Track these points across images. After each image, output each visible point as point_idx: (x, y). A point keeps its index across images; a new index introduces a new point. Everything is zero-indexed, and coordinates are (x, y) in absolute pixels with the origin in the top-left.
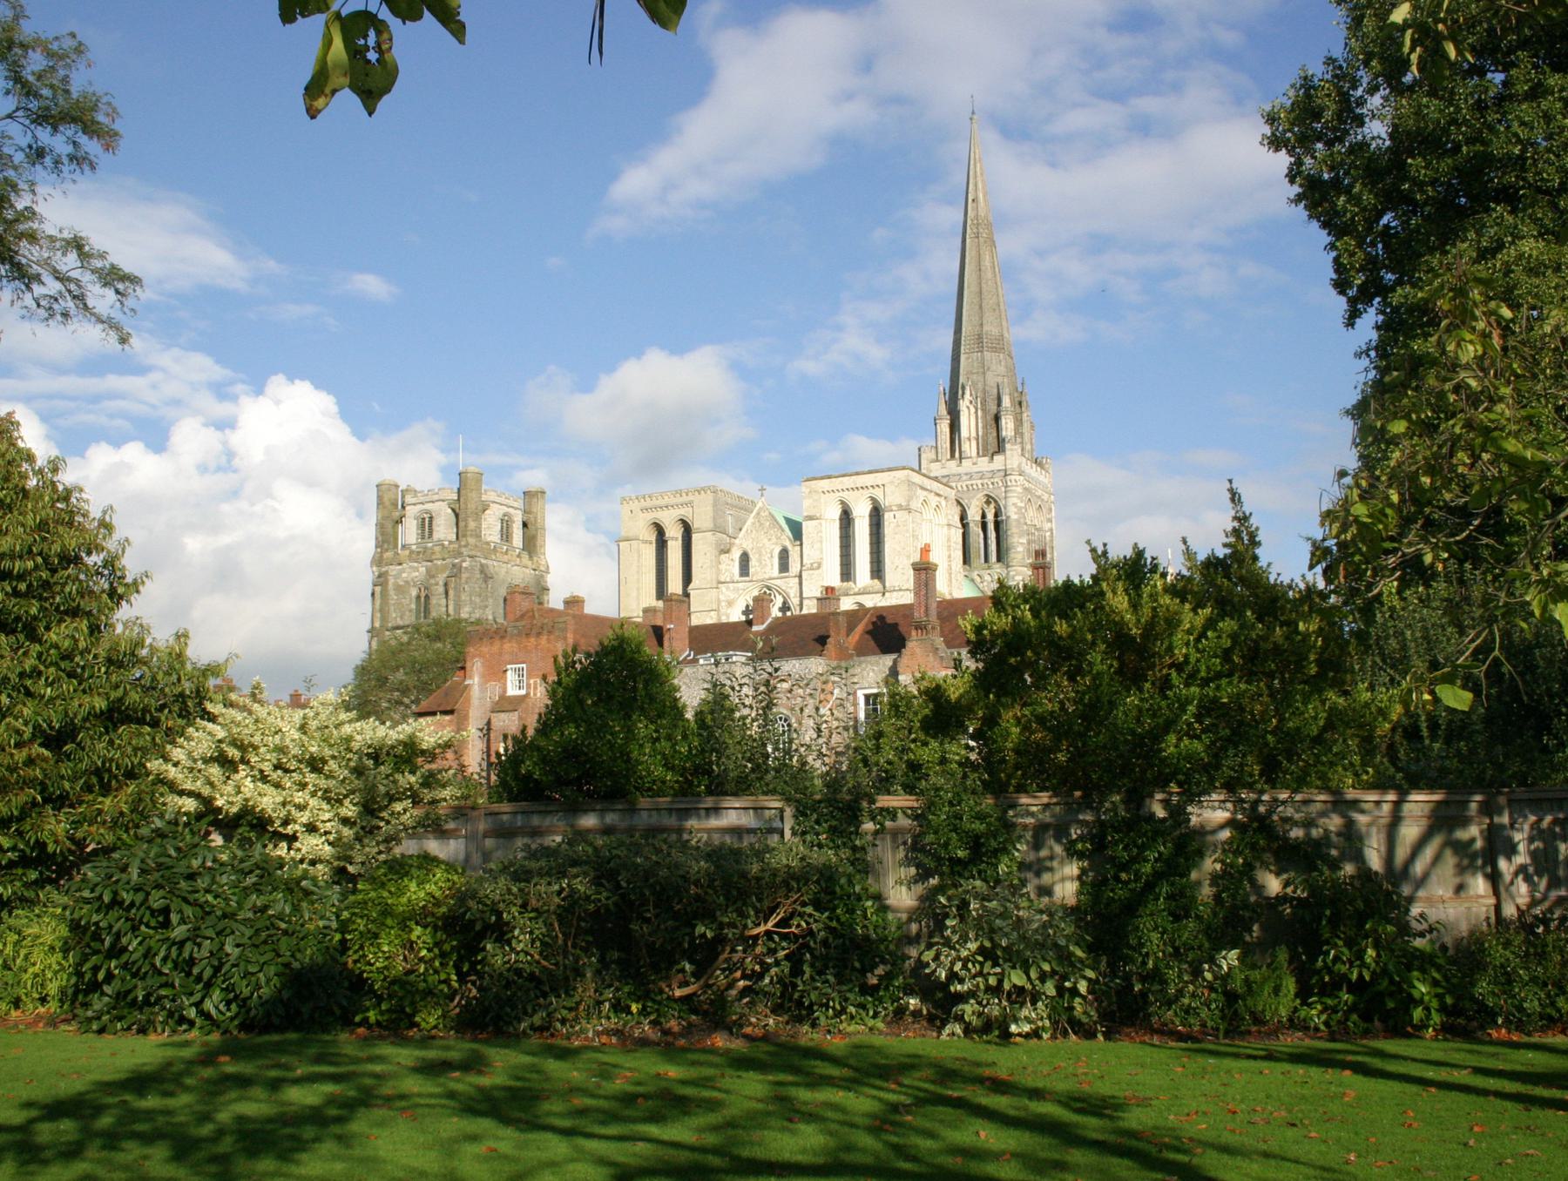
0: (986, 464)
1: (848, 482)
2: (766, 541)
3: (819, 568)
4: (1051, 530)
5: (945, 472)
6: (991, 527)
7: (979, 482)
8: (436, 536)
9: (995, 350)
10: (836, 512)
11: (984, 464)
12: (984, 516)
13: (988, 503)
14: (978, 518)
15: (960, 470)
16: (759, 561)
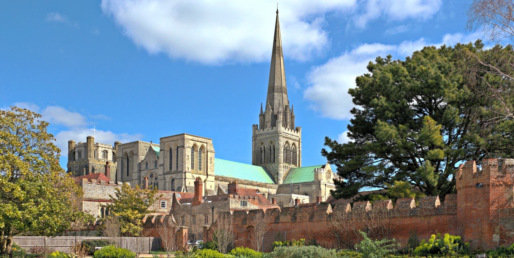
0: (271, 130)
1: (170, 139)
2: (151, 158)
3: (162, 166)
4: (299, 151)
5: (259, 133)
6: (272, 150)
7: (269, 136)
8: (82, 157)
9: (277, 92)
10: (167, 149)
11: (270, 131)
12: (270, 147)
13: (271, 143)
14: (269, 148)
15: (264, 132)
16: (150, 164)
